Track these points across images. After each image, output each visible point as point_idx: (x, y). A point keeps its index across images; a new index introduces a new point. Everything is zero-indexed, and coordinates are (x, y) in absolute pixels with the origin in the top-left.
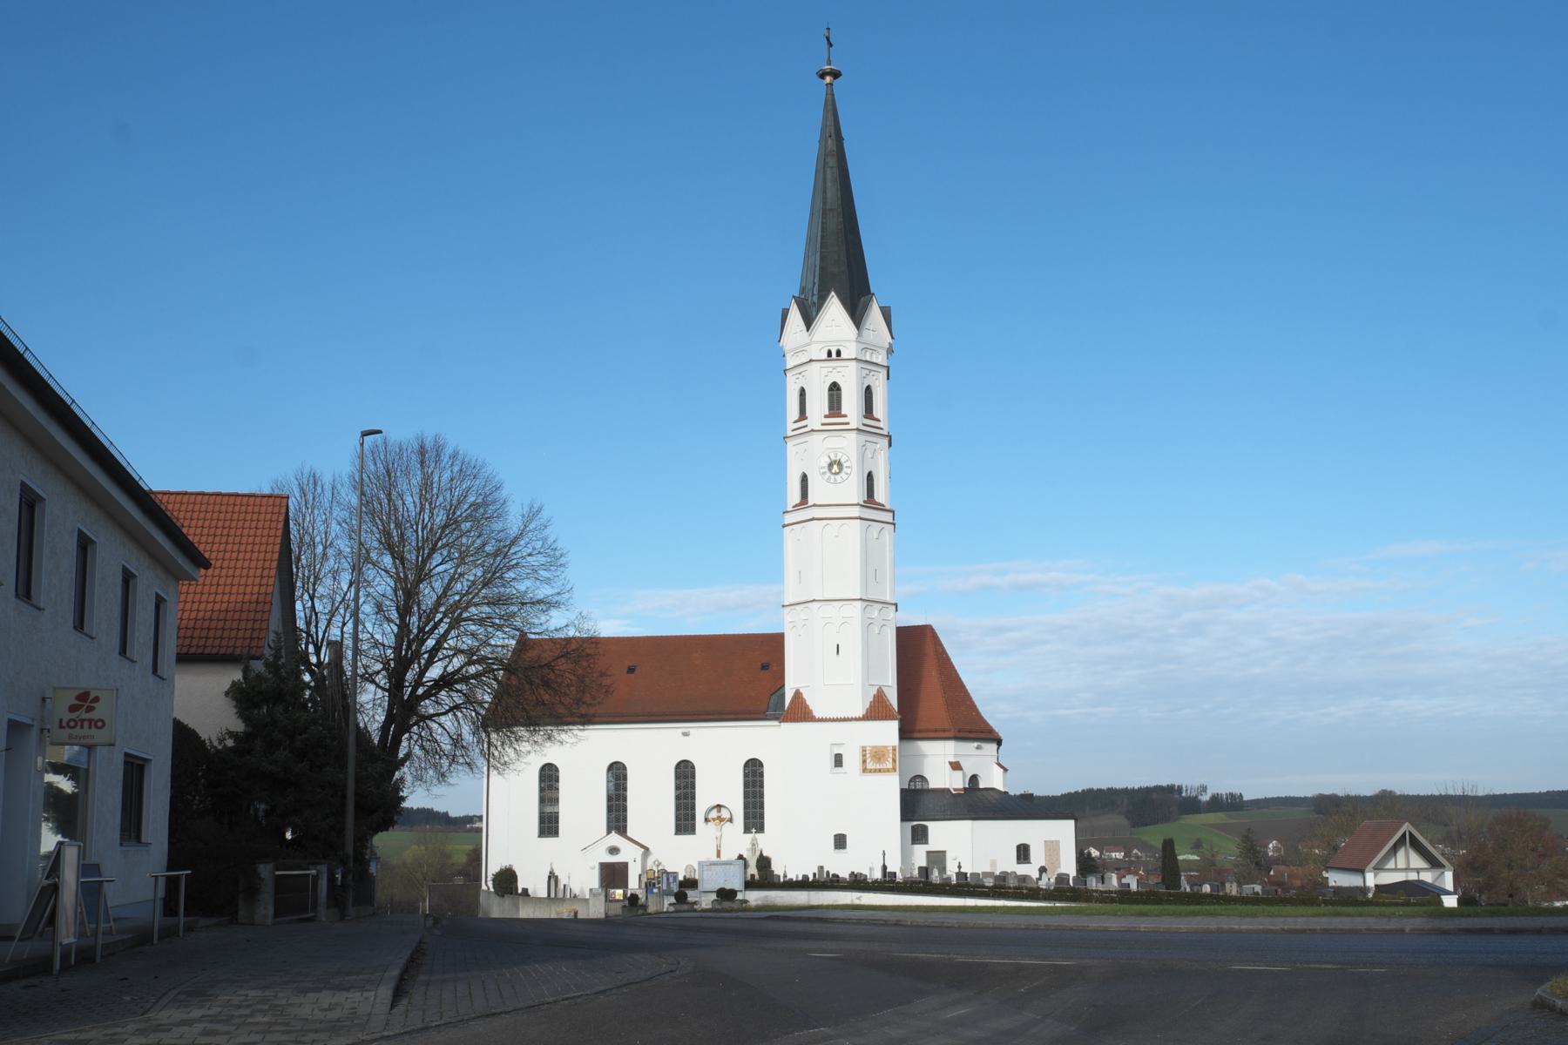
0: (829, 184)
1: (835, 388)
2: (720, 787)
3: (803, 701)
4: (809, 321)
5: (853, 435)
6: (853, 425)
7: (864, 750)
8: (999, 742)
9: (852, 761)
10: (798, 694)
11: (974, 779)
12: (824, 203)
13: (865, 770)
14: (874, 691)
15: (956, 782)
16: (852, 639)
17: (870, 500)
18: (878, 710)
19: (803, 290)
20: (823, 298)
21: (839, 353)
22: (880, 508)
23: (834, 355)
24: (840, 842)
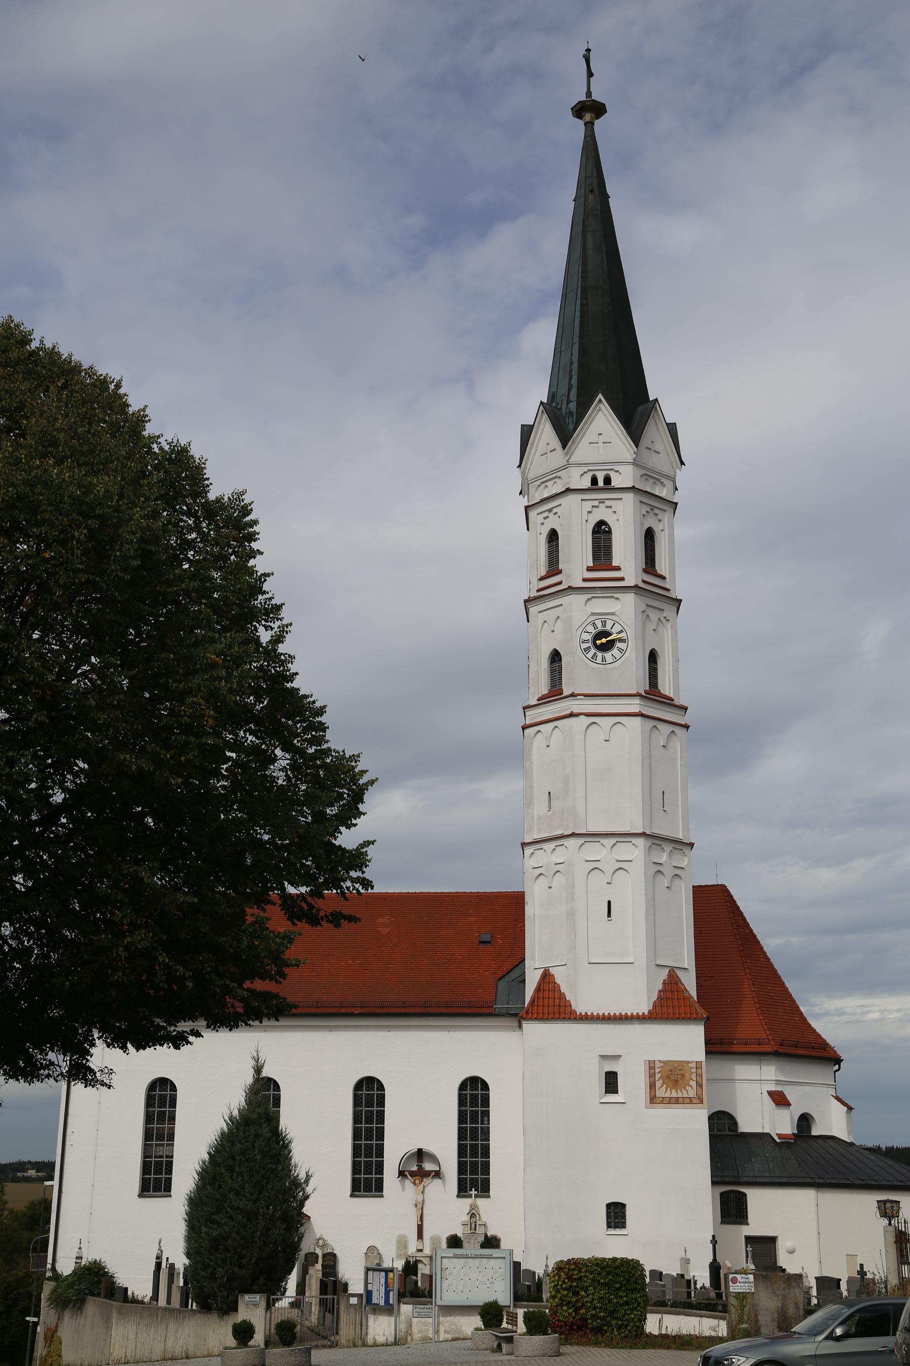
1: (602, 532)
2: (421, 1121)
3: (556, 988)
4: (565, 437)
5: (629, 599)
6: (630, 581)
7: (651, 1065)
8: (838, 1061)
9: (633, 1082)
10: (547, 977)
11: (805, 1120)
12: (584, 279)
13: (653, 1099)
14: (664, 974)
15: (782, 1124)
16: (630, 893)
17: (653, 693)
18: (669, 1006)
19: (552, 396)
21: (607, 480)
22: (667, 702)
23: (601, 485)
24: (616, 1215)
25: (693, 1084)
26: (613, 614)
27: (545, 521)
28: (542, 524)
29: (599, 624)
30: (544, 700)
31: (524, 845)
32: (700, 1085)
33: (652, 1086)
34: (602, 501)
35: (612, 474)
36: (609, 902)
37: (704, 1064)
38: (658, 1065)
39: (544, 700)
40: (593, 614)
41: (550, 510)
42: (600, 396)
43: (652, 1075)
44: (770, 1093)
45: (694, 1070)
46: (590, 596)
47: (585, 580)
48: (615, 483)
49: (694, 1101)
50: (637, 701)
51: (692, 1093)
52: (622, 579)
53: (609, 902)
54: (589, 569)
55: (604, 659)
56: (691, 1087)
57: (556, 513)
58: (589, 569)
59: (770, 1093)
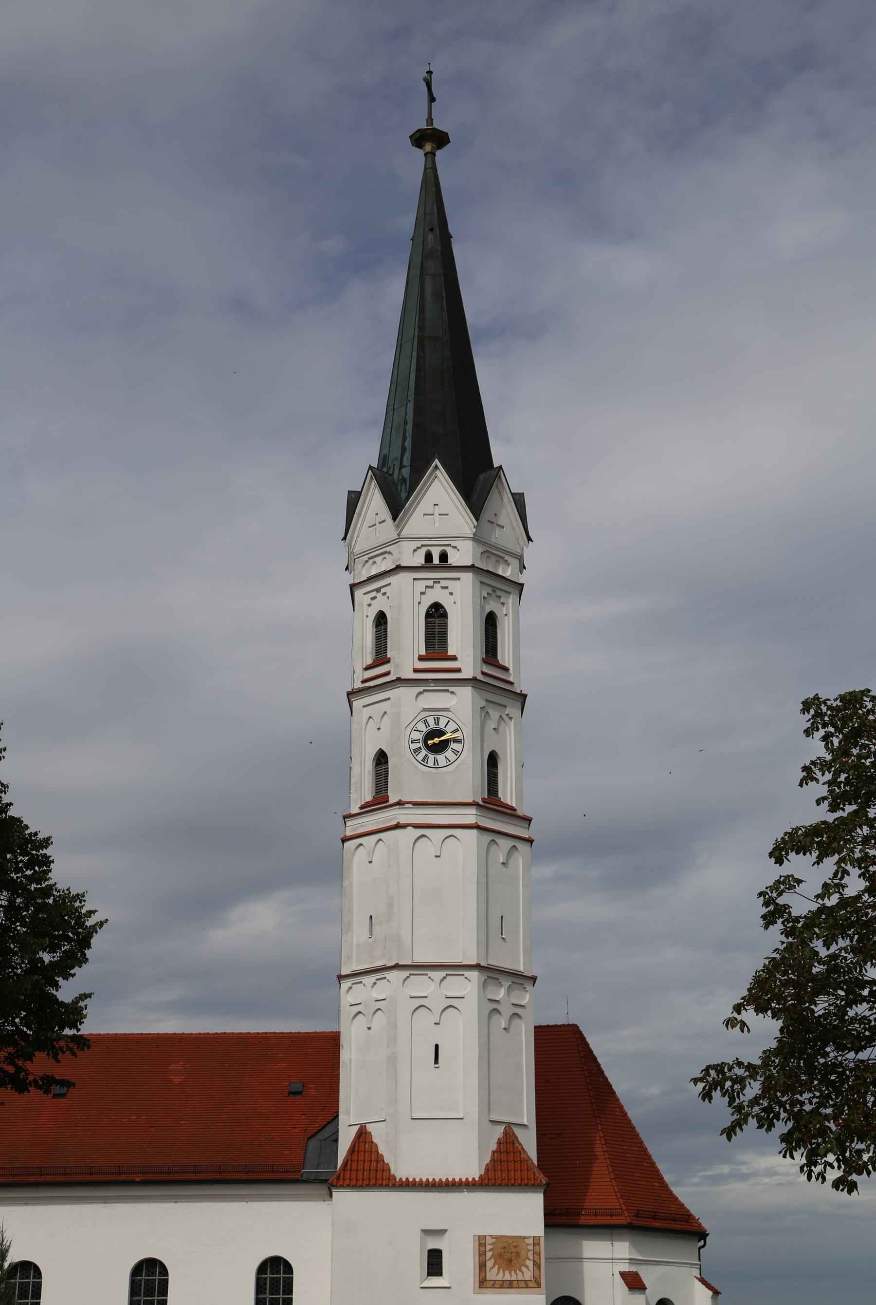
0: (429, 298)
1: (436, 615)
4: (397, 506)
5: (467, 692)
6: (467, 674)
7: (481, 1241)
8: (702, 1235)
9: (460, 1262)
10: (363, 1135)
13: (483, 1283)
14: (501, 1129)
16: (461, 1034)
17: (491, 802)
18: (503, 1170)
19: (384, 459)
20: (418, 471)
21: (444, 557)
22: (508, 812)
23: (437, 563)
25: (530, 1263)
26: (447, 710)
27: (373, 602)
28: (369, 605)
29: (431, 721)
30: (367, 808)
31: (341, 978)
32: (537, 1265)
33: (482, 1266)
34: (437, 581)
35: (449, 550)
36: (437, 1046)
37: (542, 1240)
38: (489, 1241)
39: (367, 808)
40: (424, 710)
41: (378, 590)
42: (437, 462)
43: (482, 1254)
44: (623, 1275)
45: (531, 1247)
46: (421, 689)
47: (416, 671)
48: (452, 560)
49: (531, 1284)
50: (473, 811)
51: (528, 1275)
52: (458, 670)
53: (437, 1046)
54: (421, 658)
55: (436, 761)
56: (527, 1267)
57: (384, 594)
58: (421, 658)
59: (623, 1275)
